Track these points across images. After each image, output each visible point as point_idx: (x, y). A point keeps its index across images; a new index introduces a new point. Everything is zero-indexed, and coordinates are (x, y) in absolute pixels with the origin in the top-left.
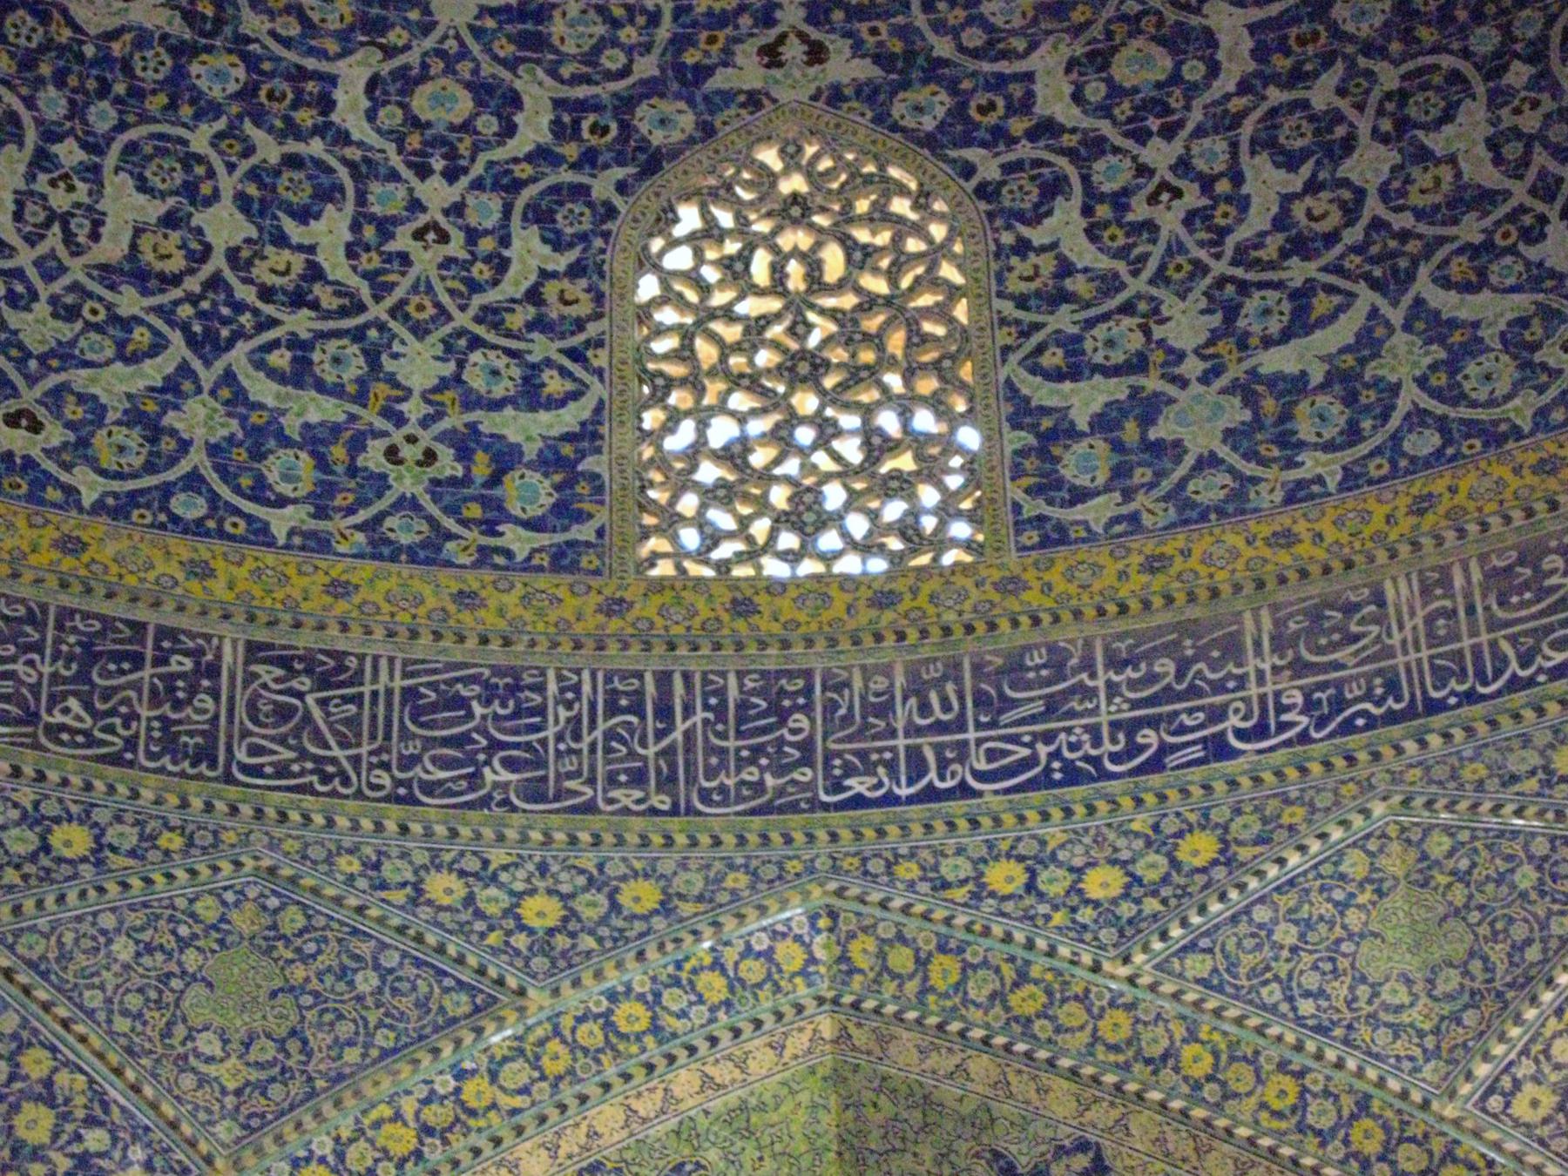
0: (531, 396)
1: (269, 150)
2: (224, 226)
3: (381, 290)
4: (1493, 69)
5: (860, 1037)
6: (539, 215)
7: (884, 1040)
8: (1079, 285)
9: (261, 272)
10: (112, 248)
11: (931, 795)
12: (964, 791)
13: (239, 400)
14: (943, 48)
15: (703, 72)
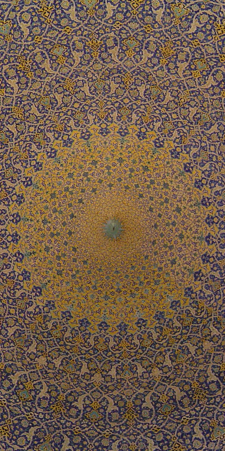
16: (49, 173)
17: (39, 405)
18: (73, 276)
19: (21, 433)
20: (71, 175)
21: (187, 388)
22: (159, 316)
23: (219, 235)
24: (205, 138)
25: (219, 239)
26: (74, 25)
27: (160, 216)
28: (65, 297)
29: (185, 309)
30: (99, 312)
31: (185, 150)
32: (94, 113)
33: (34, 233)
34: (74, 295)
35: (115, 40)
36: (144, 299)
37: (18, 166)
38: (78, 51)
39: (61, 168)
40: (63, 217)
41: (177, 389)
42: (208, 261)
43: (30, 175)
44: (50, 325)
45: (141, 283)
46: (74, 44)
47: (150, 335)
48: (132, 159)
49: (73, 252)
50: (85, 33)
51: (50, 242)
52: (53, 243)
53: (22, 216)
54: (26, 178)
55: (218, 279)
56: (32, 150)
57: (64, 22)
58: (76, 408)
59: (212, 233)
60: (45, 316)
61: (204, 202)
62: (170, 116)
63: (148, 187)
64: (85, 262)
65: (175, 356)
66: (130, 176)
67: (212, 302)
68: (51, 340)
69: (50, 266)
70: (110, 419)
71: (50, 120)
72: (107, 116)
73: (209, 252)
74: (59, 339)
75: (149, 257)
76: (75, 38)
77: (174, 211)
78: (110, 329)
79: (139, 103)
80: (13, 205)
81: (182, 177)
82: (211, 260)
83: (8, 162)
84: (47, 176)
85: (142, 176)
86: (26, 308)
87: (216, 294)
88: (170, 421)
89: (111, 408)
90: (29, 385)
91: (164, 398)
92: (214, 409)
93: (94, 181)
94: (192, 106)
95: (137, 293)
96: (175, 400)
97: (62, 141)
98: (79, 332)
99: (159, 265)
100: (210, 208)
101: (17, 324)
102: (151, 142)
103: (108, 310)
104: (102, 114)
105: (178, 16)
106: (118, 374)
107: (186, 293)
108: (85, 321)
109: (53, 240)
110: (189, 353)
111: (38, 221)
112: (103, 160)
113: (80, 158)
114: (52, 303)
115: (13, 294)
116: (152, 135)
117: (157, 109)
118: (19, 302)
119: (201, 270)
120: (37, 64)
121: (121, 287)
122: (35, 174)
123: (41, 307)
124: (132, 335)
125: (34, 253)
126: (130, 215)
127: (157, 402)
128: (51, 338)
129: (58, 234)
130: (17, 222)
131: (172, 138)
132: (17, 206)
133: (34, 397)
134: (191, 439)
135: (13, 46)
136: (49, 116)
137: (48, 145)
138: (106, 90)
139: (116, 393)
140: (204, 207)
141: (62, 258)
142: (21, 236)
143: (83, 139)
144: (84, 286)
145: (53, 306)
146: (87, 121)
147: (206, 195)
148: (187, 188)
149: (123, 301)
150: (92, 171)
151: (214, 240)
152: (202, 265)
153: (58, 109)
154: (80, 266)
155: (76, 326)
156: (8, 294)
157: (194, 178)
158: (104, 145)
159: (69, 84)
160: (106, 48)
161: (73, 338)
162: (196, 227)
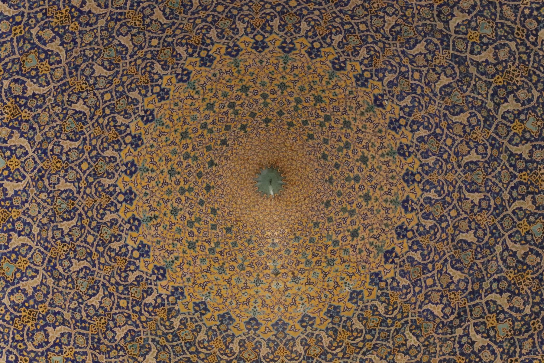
16: (180, 104)
18: (212, 250)
20: (210, 106)
22: (333, 312)
23: (422, 200)
24: (405, 61)
25: (422, 205)
27: (337, 166)
28: (198, 281)
29: (369, 304)
30: (247, 302)
31: (376, 76)
32: (246, 19)
33: (156, 188)
34: (212, 277)
36: (311, 286)
37: (134, 95)
39: (196, 96)
40: (198, 166)
42: (405, 236)
43: (151, 107)
44: (176, 323)
45: (308, 262)
47: (319, 340)
49: (212, 216)
51: (179, 200)
52: (183, 202)
53: (139, 165)
54: (146, 112)
55: (419, 263)
56: (154, 71)
59: (412, 197)
60: (170, 310)
61: (402, 152)
62: (356, 27)
63: (322, 125)
64: (229, 230)
66: (296, 109)
67: (409, 296)
68: (177, 345)
69: (178, 236)
71: (182, 29)
72: (264, 24)
73: (406, 223)
74: (190, 343)
75: (320, 225)
77: (357, 160)
78: (262, 329)
80: (126, 149)
81: (372, 113)
82: (410, 234)
83: (120, 89)
84: (176, 108)
85: (312, 110)
86: (143, 298)
87: (415, 284)
93: (244, 115)
94: (388, 15)
95: (302, 277)
97: (198, 59)
98: (219, 332)
99: (334, 237)
100: (409, 160)
101: (129, 322)
102: (328, 62)
103: (259, 301)
104: (258, 21)
107: (372, 281)
108: (227, 316)
109: (183, 198)
111: (162, 172)
112: (258, 85)
113: (224, 82)
114: (180, 290)
115: (125, 278)
116: (329, 53)
117: (338, 16)
118: (133, 290)
119: (393, 249)
121: (278, 267)
122: (159, 104)
123: (164, 297)
124: (293, 339)
125: (156, 217)
126: (294, 163)
128: (178, 342)
129: (190, 190)
130: (131, 174)
131: (358, 58)
132: (132, 150)
136: (180, 24)
137: (178, 64)
140: (402, 158)
141: (196, 225)
142: (137, 193)
143: (228, 57)
144: (227, 265)
145: (182, 294)
146: (235, 30)
147: (404, 141)
148: (377, 129)
149: (282, 286)
150: (241, 101)
151: (415, 206)
152: (395, 240)
153: (193, 13)
154: (222, 236)
155: (214, 324)
156: (118, 278)
157: (388, 116)
158: (259, 64)
161: (208, 341)
162: (388, 186)
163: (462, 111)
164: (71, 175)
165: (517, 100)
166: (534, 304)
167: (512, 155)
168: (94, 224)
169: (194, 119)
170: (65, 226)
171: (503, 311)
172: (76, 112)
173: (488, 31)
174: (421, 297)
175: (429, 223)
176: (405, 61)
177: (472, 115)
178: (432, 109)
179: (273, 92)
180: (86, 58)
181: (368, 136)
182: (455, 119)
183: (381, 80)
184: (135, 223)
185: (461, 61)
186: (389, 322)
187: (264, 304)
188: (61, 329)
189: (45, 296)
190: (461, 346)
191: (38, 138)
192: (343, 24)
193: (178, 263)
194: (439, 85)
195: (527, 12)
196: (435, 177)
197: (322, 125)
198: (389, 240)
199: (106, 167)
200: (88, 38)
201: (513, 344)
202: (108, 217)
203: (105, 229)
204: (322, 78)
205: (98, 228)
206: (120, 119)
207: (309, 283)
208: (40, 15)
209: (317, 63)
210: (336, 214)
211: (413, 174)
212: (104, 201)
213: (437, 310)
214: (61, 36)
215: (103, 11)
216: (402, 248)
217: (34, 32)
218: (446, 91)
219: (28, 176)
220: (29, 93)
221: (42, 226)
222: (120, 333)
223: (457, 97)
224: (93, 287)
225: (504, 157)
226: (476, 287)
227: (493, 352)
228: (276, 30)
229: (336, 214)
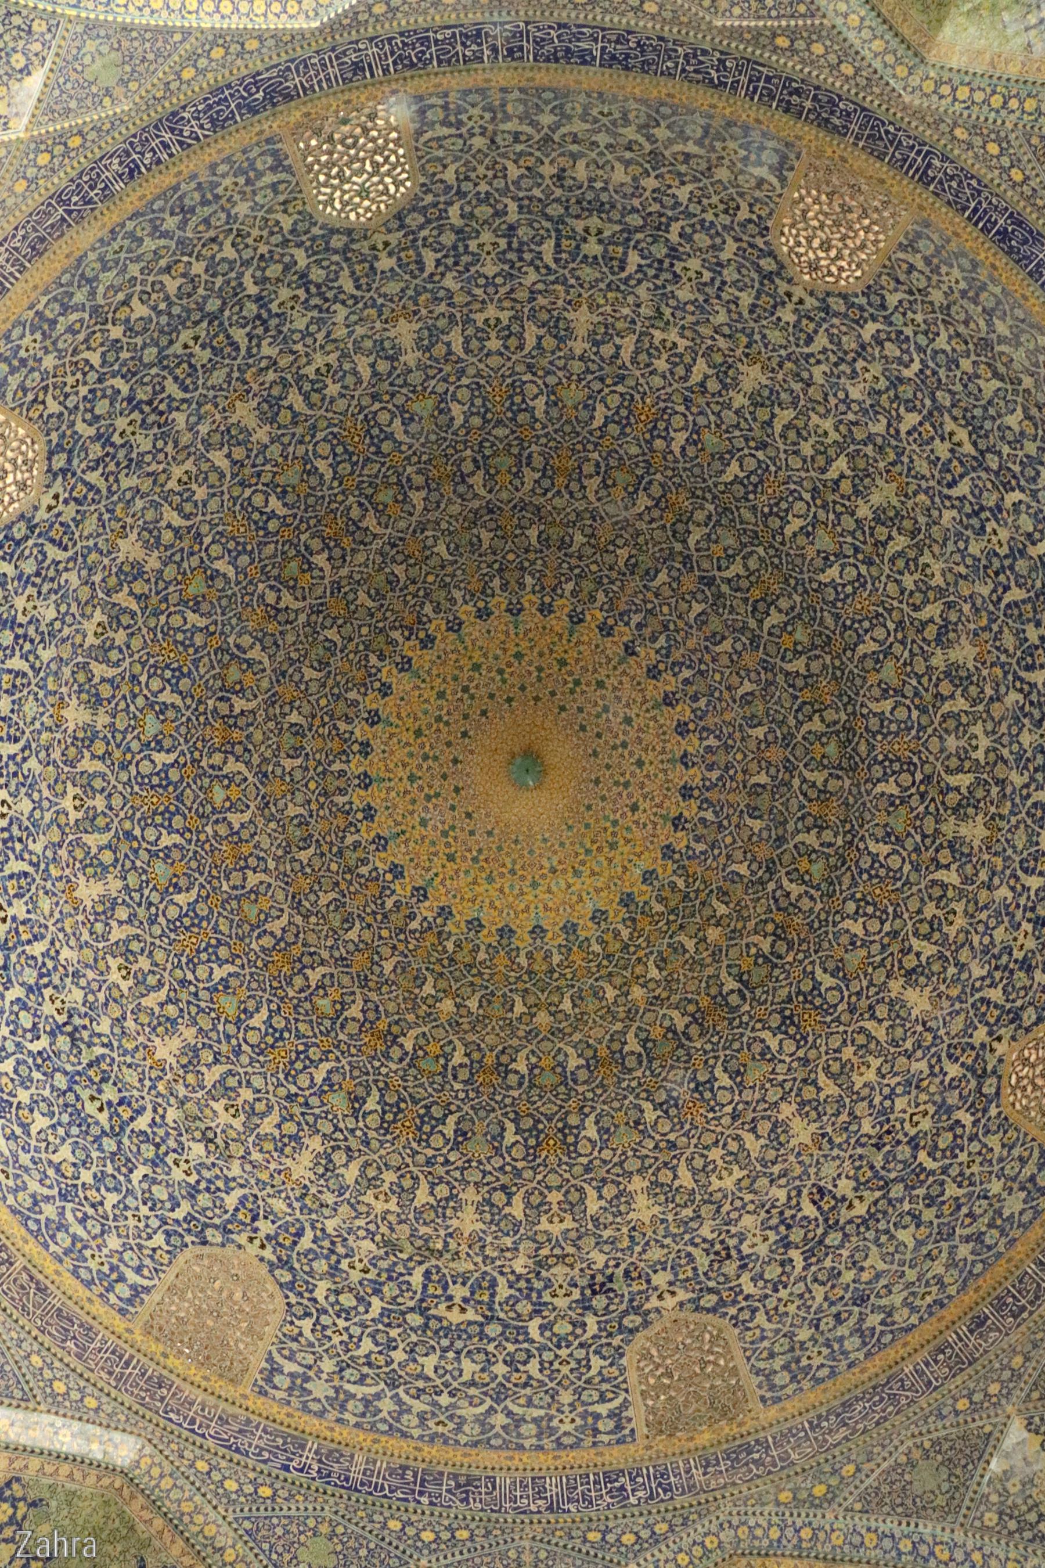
0: (138, 1270)
1: (109, 1169)
2: (86, 1176)
3: (115, 1220)
4: (445, 1350)
5: (126, 1492)
6: (168, 1234)
7: (132, 1497)
8: (302, 1340)
9: (88, 1193)
10: (56, 1158)
11: (193, 1431)
12: (203, 1436)
13: (62, 1213)
14: (297, 1266)
15: (231, 1232)
17: (455, 1077)
18: (475, 860)
19: (433, 1127)
20: (441, 695)
21: (691, 1008)
22: (627, 901)
26: (404, 448)
35: (475, 460)
37: (352, 695)
38: (418, 489)
41: (675, 1014)
43: (374, 706)
44: (450, 946)
45: (588, 852)
46: (409, 480)
47: (617, 934)
48: (536, 650)
50: (424, 458)
53: (374, 776)
57: (386, 447)
58: (516, 1072)
59: (690, 749)
60: (440, 933)
63: (572, 692)
64: (490, 833)
65: (664, 960)
70: (575, 1081)
76: (409, 469)
78: (550, 935)
79: (532, 556)
80: (355, 760)
82: (696, 793)
83: (336, 691)
88: (672, 1067)
89: (573, 1063)
90: (433, 1049)
91: (657, 1032)
92: (742, 1035)
93: (481, 698)
96: (675, 1032)
100: (679, 708)
105: (570, 403)
106: (574, 1006)
107: (664, 855)
110: (685, 951)
116: (563, 605)
118: (393, 917)
120: (354, 523)
127: (647, 1040)
129: (437, 795)
130: (366, 787)
133: (445, 1067)
134: (712, 1090)
135: (311, 501)
138: (475, 545)
139: (577, 1037)
146: (453, 601)
147: (668, 688)
149: (563, 886)
155: (493, 940)
159: (413, 547)
160: (462, 476)
163: (724, 638)
164: (299, 798)
165: (780, 611)
166: (845, 833)
167: (788, 674)
168: (335, 849)
169: (426, 713)
170: (304, 856)
171: (814, 851)
172: (292, 725)
173: (731, 541)
174: (722, 860)
175: (714, 775)
176: (650, 595)
177: (736, 640)
178: (691, 643)
179: (509, 665)
180: (292, 662)
181: (627, 692)
182: (718, 649)
183: (627, 624)
184: (381, 842)
185: (710, 582)
186: (692, 895)
187: (546, 908)
188: (321, 970)
189: (297, 936)
190: (776, 901)
191: (256, 760)
192: (571, 569)
193: (439, 879)
194: (692, 615)
195: (766, 510)
196: (710, 721)
197: (572, 692)
198: (675, 805)
199: (336, 783)
200: (290, 638)
201: (831, 883)
202: (350, 840)
203: (348, 853)
204: (561, 636)
205: (340, 853)
206: (342, 726)
207: (593, 874)
208: (234, 621)
209: (552, 621)
210: (609, 790)
211: (686, 724)
212: (341, 822)
213: (743, 869)
214: (261, 641)
215: (301, 604)
216: (690, 810)
217: (231, 640)
218: (702, 620)
219: (252, 805)
220: (237, 711)
221: (277, 859)
222: (388, 966)
223: (715, 624)
224: (348, 921)
225: (780, 679)
226: (780, 832)
227: (812, 898)
228: (498, 591)
229: (609, 790)
